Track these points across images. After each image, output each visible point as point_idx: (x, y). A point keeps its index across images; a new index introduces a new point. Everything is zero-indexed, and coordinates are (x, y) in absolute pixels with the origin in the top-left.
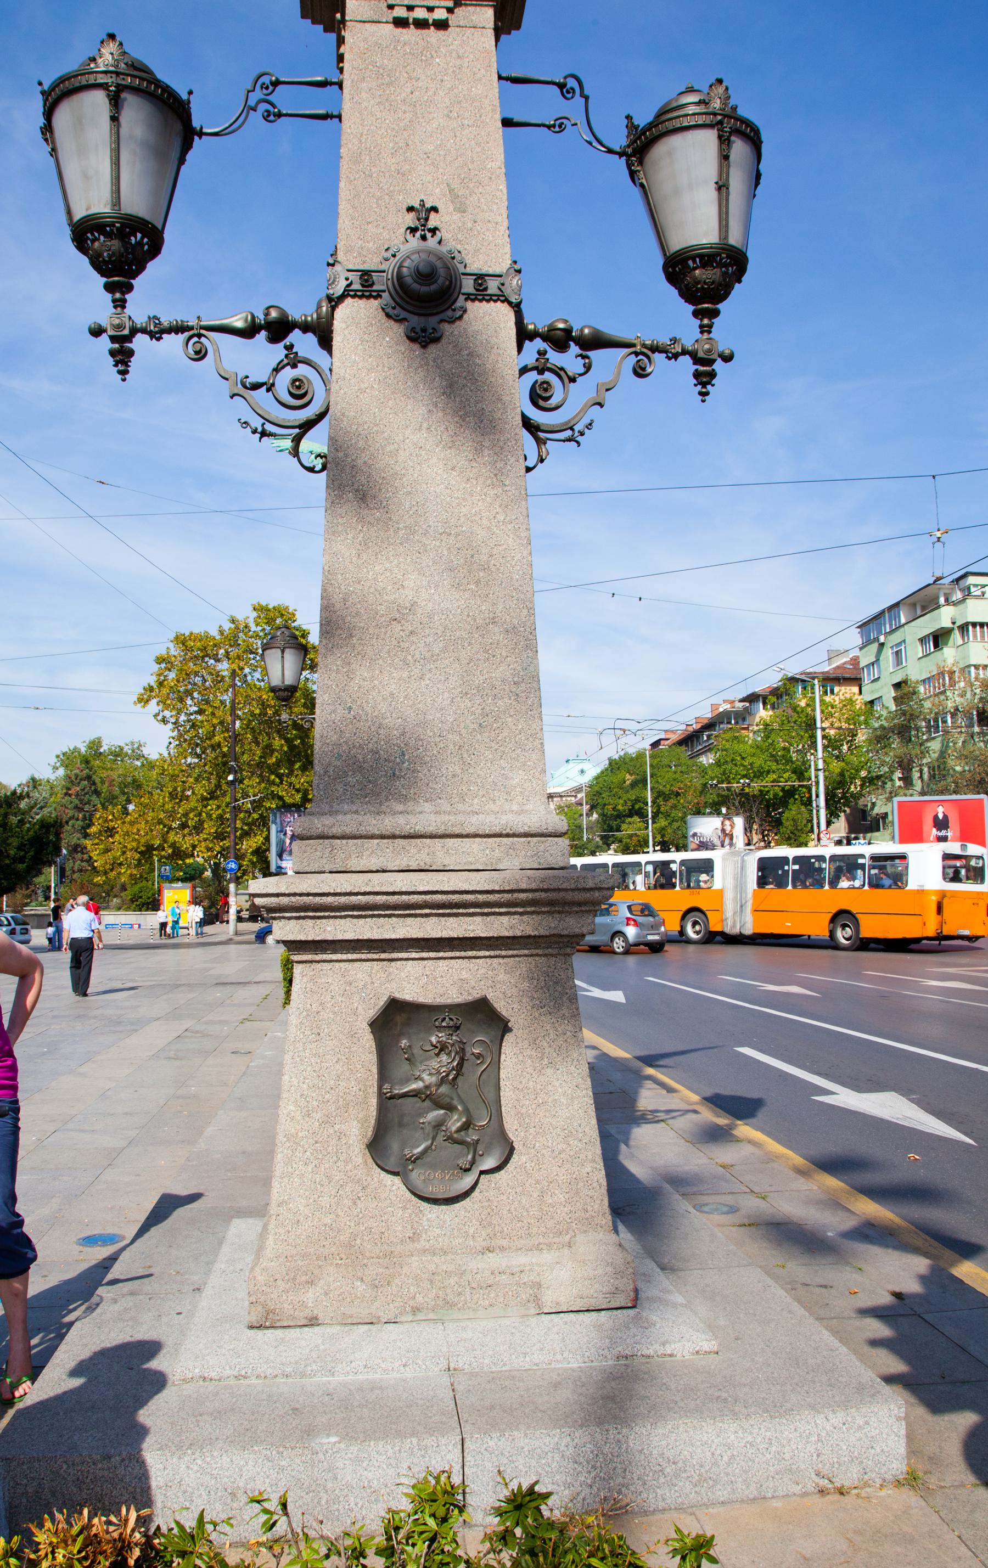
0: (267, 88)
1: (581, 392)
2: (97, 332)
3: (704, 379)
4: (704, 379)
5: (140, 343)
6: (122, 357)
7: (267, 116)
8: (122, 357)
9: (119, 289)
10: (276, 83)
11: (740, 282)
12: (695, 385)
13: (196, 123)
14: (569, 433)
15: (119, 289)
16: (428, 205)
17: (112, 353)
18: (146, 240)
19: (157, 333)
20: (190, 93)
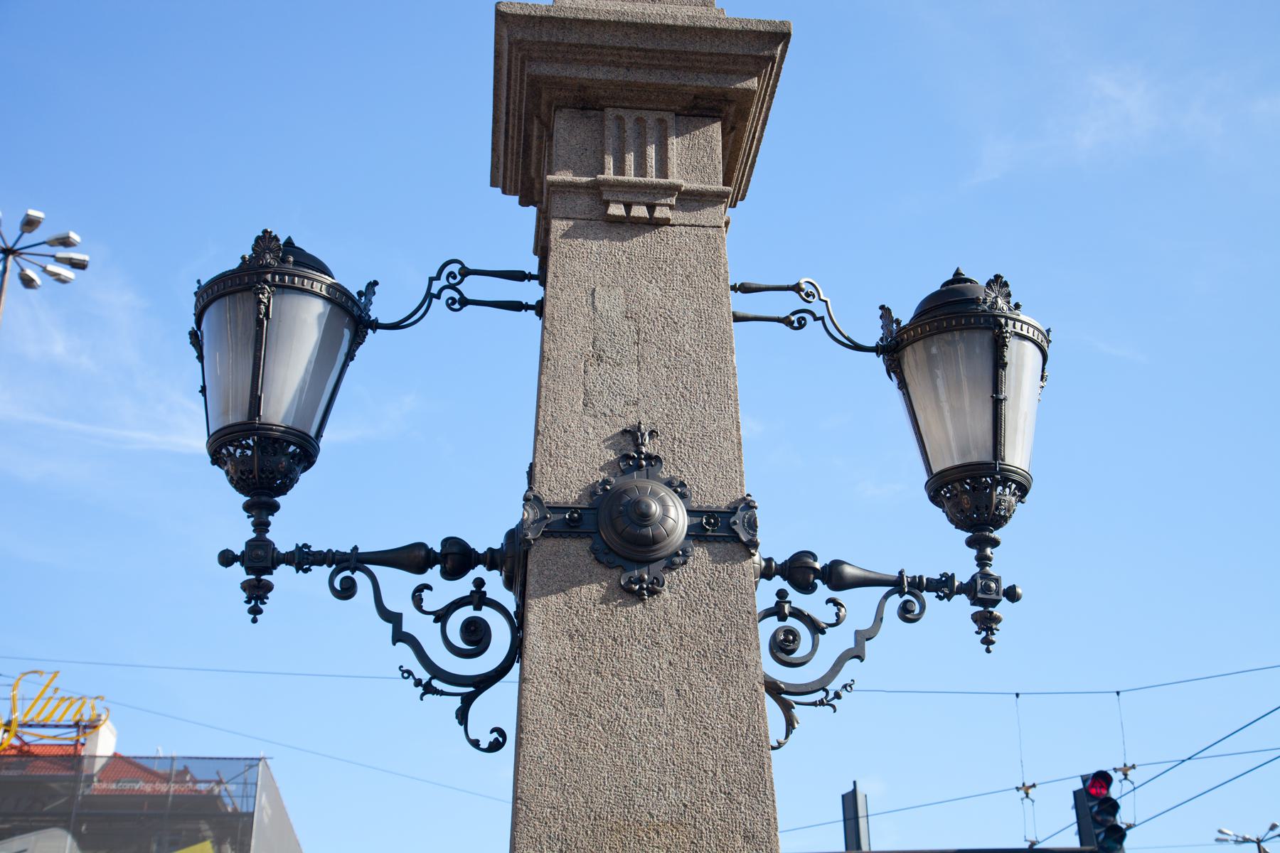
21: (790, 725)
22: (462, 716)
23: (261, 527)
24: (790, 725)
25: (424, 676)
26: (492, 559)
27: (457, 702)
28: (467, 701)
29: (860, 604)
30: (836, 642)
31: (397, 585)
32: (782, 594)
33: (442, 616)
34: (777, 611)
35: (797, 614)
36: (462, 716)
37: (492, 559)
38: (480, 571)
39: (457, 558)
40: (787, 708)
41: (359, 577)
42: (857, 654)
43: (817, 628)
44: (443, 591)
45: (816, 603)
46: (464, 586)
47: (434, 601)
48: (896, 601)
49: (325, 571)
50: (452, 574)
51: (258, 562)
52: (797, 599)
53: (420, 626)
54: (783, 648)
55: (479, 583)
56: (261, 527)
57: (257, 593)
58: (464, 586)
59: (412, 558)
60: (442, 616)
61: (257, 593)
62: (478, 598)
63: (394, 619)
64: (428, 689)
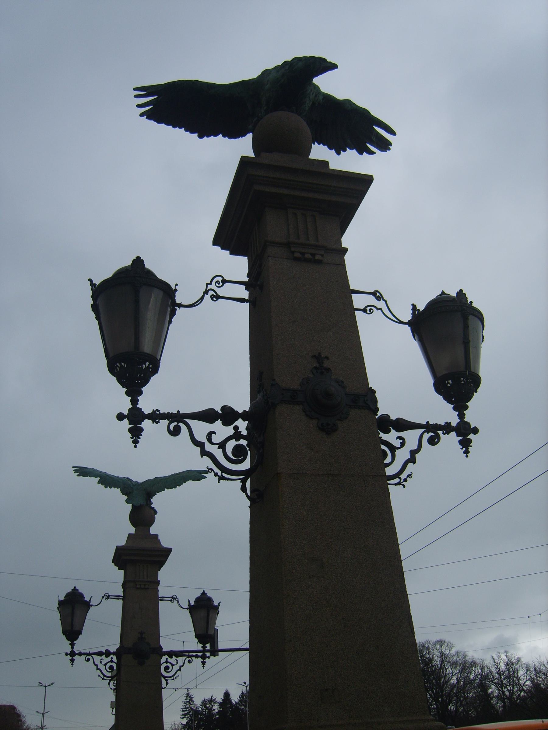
0: (219, 284)
1: (402, 455)
2: (120, 417)
3: (466, 444)
4: (466, 444)
5: (146, 424)
6: (136, 433)
7: (212, 297)
8: (136, 433)
9: (134, 392)
10: (224, 281)
11: (476, 392)
12: (462, 449)
13: (178, 300)
14: (397, 480)
15: (134, 392)
16: (323, 355)
17: (130, 430)
18: (151, 366)
19: (156, 417)
20: (177, 285)
21: (167, 683)
22: (109, 684)
23: (72, 648)
24: (167, 683)
25: (102, 676)
26: (114, 653)
27: (108, 681)
28: (110, 681)
29: (181, 659)
30: (176, 667)
31: (97, 658)
32: (167, 659)
33: (105, 665)
34: (167, 662)
35: (170, 663)
36: (109, 684)
37: (114, 653)
38: (112, 656)
39: (108, 653)
40: (166, 680)
41: (90, 657)
42: (180, 670)
43: (173, 665)
44: (106, 660)
45: (173, 660)
46: (109, 659)
47: (104, 662)
48: (188, 659)
49: (84, 656)
50: (107, 656)
51: (73, 654)
52: (169, 660)
53: (101, 667)
54: (167, 668)
55: (112, 658)
56: (72, 648)
57: (72, 661)
58: (109, 659)
59: (100, 654)
60: (105, 665)
61: (72, 661)
62: (112, 661)
63: (97, 666)
64: (103, 679)
